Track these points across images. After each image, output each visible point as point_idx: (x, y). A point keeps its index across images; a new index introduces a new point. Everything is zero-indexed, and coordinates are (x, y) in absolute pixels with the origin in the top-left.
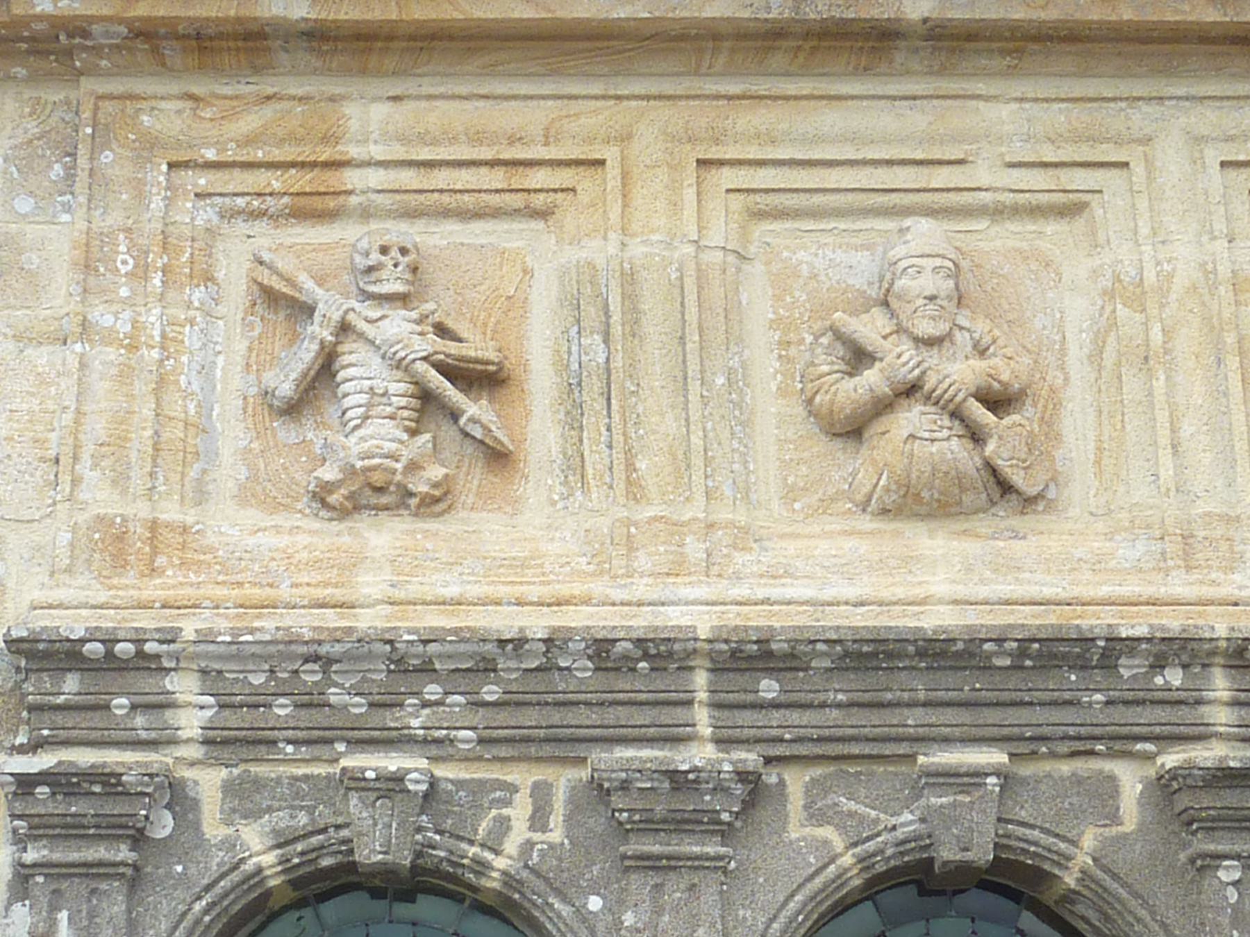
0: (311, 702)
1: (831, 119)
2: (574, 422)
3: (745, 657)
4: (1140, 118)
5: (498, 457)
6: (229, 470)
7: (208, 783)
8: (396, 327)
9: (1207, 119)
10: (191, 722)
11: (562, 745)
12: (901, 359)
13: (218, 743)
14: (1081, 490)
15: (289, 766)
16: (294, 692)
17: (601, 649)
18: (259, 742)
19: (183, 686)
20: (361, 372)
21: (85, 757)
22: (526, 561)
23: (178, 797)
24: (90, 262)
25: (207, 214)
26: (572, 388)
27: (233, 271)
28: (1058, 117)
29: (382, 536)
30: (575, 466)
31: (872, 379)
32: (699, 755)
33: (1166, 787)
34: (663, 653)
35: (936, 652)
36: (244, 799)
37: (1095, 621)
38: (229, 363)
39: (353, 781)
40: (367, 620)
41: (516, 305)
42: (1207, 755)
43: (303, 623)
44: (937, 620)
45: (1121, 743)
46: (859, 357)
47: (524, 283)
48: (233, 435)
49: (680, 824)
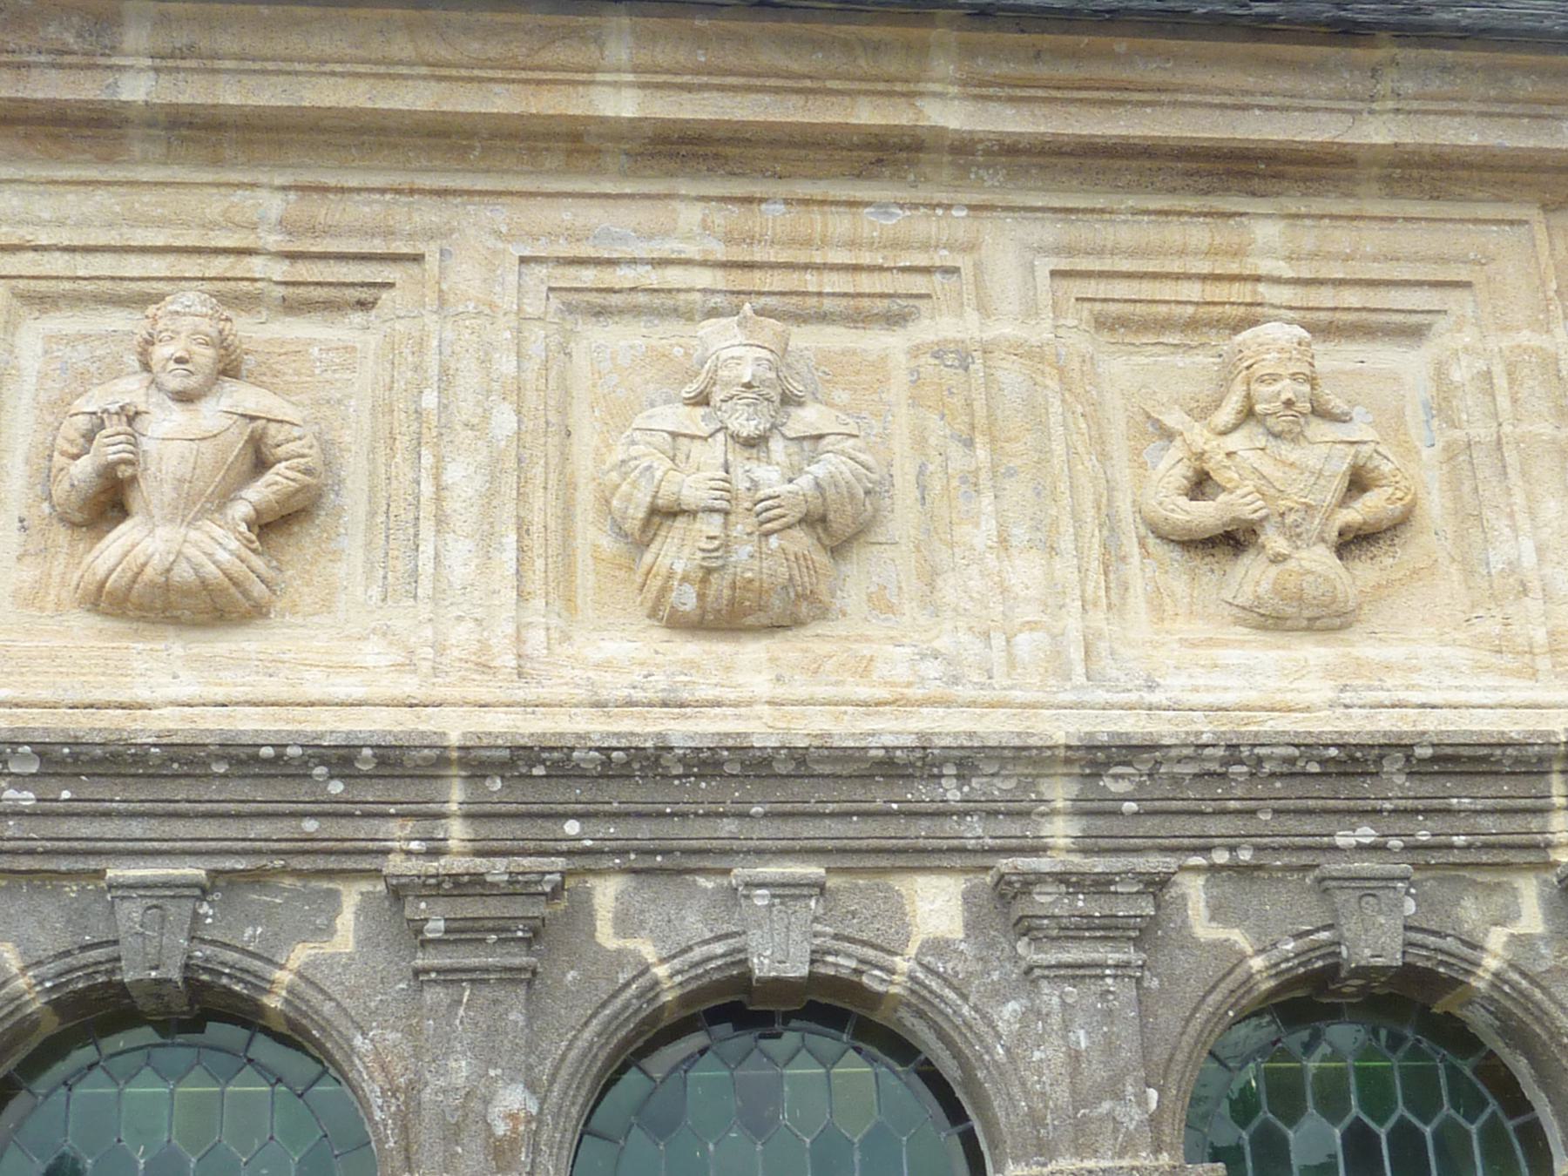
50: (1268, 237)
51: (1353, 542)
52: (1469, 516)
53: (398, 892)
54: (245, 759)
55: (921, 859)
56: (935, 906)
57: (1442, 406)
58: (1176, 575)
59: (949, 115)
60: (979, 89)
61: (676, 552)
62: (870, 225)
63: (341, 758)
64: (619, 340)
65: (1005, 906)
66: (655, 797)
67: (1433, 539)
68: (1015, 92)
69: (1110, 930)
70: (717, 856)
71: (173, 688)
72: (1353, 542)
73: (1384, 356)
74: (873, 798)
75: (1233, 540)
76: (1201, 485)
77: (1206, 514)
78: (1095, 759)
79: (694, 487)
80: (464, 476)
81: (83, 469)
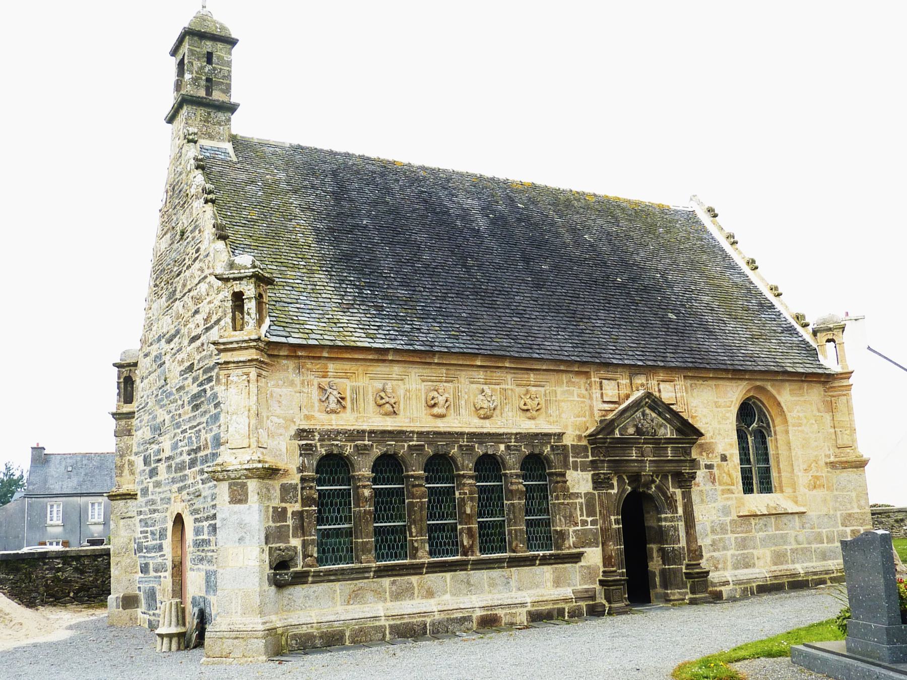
0: (329, 436)
1: (379, 369)
2: (353, 403)
3: (371, 432)
4: (410, 370)
5: (344, 407)
6: (317, 408)
7: (318, 444)
8: (335, 393)
9: (416, 370)
10: (317, 438)
11: (353, 441)
12: (387, 399)
13: (319, 440)
14: (402, 412)
15: (327, 443)
16: (327, 436)
17: (358, 431)
18: (324, 440)
19: (316, 434)
20: (332, 398)
21: (309, 442)
22: (347, 421)
23: (316, 447)
24: (303, 383)
25: (313, 377)
26: (352, 400)
27: (316, 384)
28: (402, 369)
29: (333, 416)
30: (353, 409)
31: (384, 401)
32: (366, 442)
33: (409, 446)
34: (364, 431)
35: (390, 432)
36: (322, 446)
37: (404, 429)
38: (315, 393)
39: (333, 445)
40: (335, 427)
41: (345, 389)
42: (414, 443)
43: (326, 427)
44: (389, 428)
45: (405, 441)
46: (382, 398)
47: (347, 386)
48: (317, 404)
49: (365, 450)
50: (532, 376)
51: (537, 410)
52: (547, 407)
53: (461, 446)
54: (449, 433)
55: (501, 443)
56: (502, 447)
57: (545, 395)
58: (520, 413)
59: (507, 365)
60: (510, 362)
61: (482, 412)
62: (498, 374)
63: (457, 433)
64: (474, 386)
65: (508, 448)
66: (481, 437)
67: (543, 410)
68: (513, 363)
69: (517, 450)
70: (486, 442)
71: (442, 426)
72: (537, 410)
73: (540, 389)
74: (497, 437)
75: (528, 410)
76: (525, 404)
77: (525, 408)
78: (517, 434)
79: (485, 406)
80: (463, 402)
81: (433, 402)
